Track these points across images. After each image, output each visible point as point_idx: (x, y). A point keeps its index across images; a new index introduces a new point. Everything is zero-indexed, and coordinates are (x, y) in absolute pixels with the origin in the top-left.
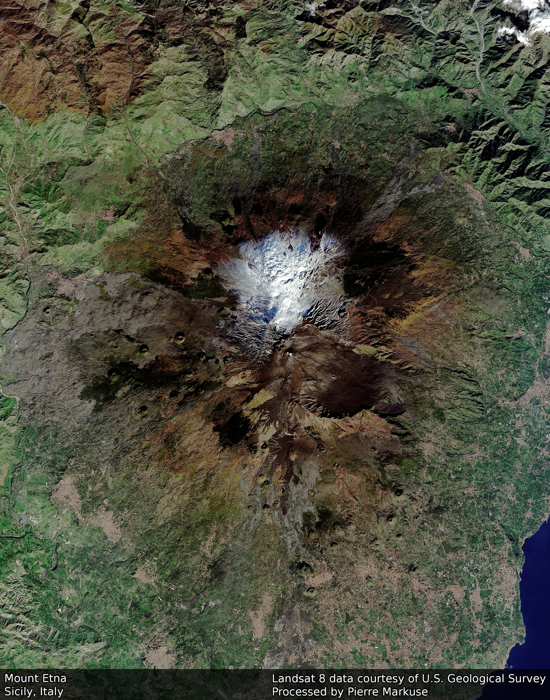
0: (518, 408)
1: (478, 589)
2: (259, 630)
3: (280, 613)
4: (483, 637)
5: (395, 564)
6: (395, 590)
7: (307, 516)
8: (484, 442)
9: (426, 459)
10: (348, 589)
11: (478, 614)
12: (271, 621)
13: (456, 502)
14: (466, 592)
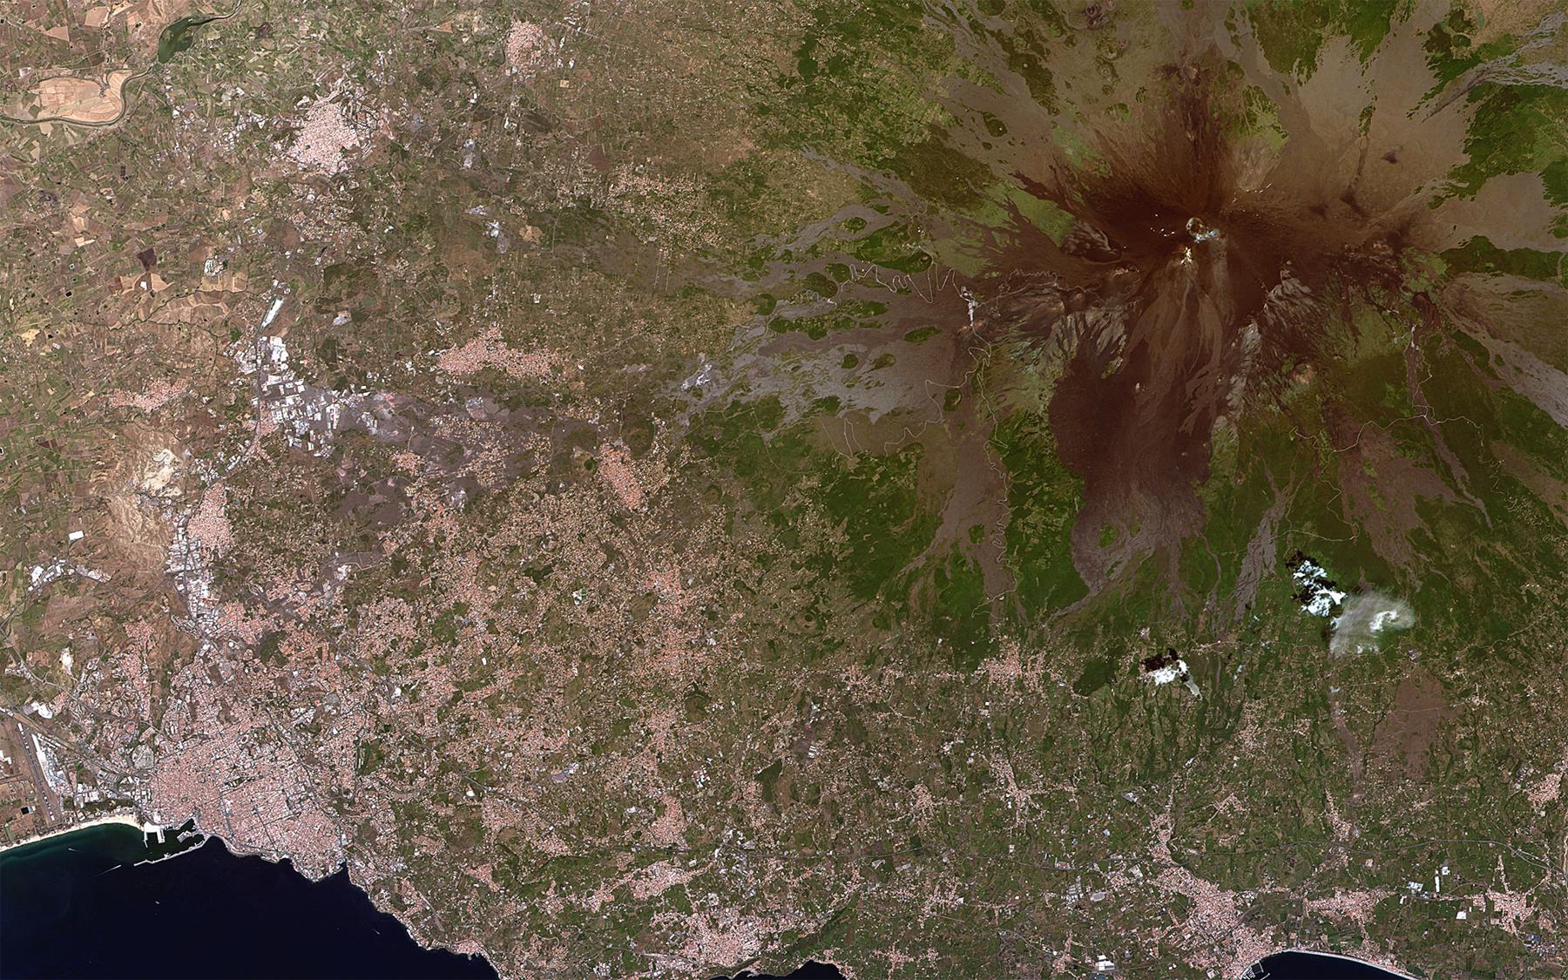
0: (1156, 870)
1: (686, 878)
2: (458, 362)
3: (513, 405)
4: (572, 915)
5: (700, 656)
6: (636, 673)
7: (771, 410)
8: (1052, 802)
9: (980, 671)
10: (612, 553)
11: (623, 895)
12: (487, 382)
13: (886, 770)
14: (671, 851)
